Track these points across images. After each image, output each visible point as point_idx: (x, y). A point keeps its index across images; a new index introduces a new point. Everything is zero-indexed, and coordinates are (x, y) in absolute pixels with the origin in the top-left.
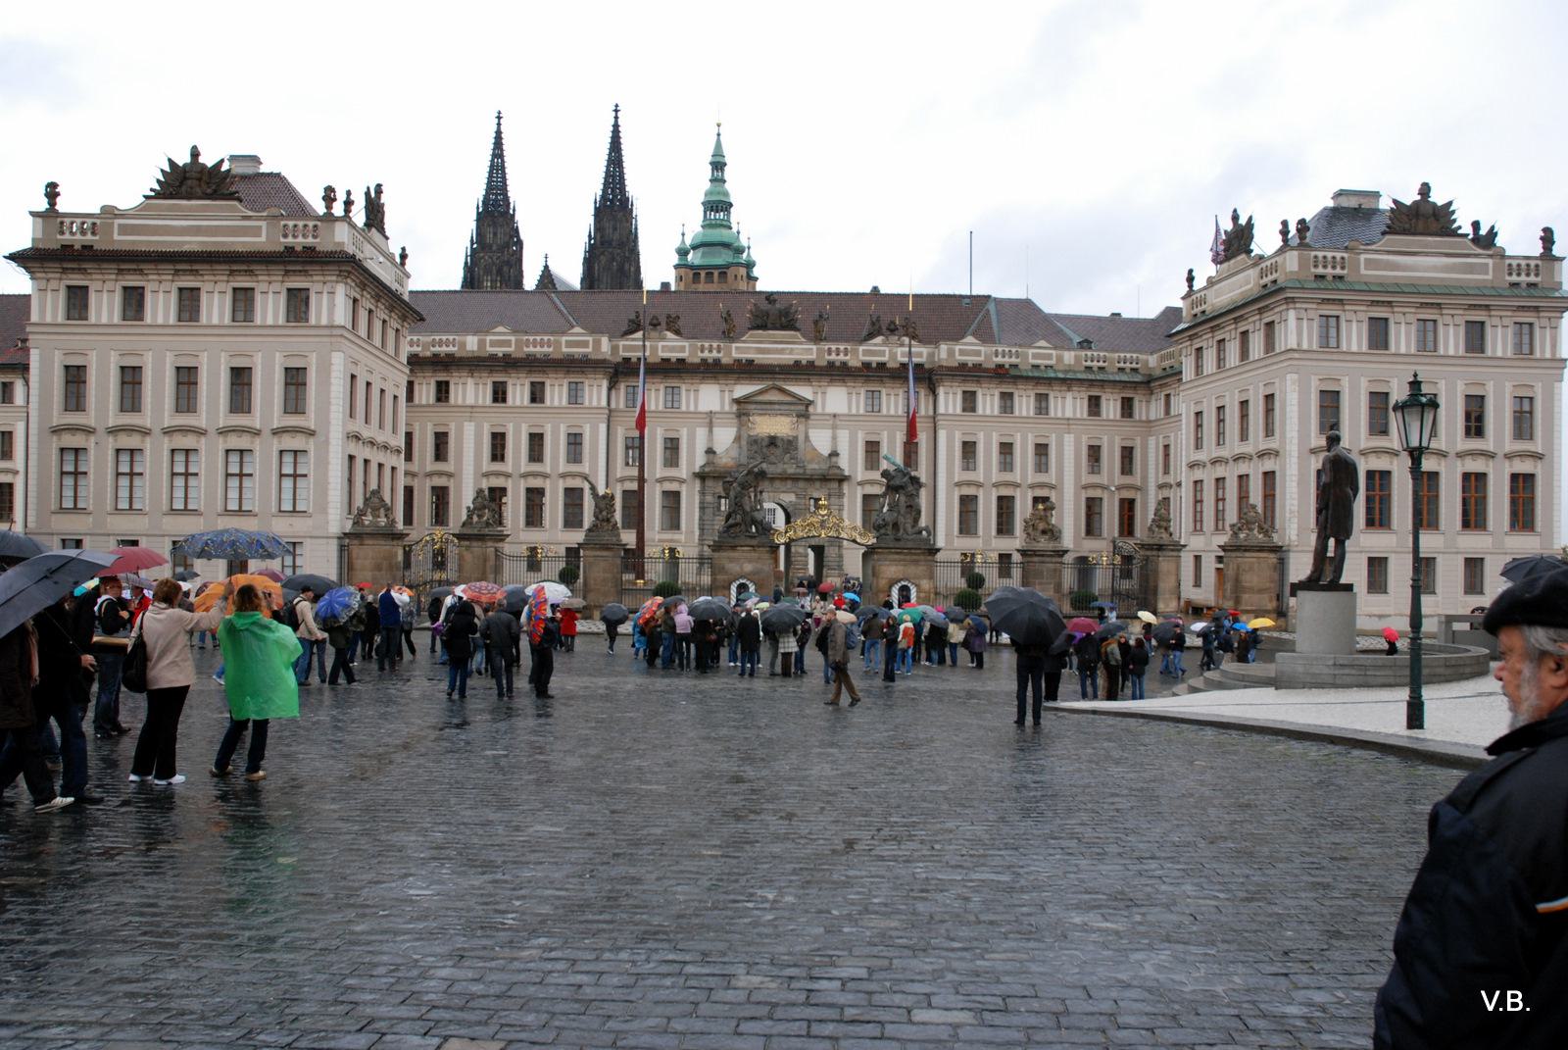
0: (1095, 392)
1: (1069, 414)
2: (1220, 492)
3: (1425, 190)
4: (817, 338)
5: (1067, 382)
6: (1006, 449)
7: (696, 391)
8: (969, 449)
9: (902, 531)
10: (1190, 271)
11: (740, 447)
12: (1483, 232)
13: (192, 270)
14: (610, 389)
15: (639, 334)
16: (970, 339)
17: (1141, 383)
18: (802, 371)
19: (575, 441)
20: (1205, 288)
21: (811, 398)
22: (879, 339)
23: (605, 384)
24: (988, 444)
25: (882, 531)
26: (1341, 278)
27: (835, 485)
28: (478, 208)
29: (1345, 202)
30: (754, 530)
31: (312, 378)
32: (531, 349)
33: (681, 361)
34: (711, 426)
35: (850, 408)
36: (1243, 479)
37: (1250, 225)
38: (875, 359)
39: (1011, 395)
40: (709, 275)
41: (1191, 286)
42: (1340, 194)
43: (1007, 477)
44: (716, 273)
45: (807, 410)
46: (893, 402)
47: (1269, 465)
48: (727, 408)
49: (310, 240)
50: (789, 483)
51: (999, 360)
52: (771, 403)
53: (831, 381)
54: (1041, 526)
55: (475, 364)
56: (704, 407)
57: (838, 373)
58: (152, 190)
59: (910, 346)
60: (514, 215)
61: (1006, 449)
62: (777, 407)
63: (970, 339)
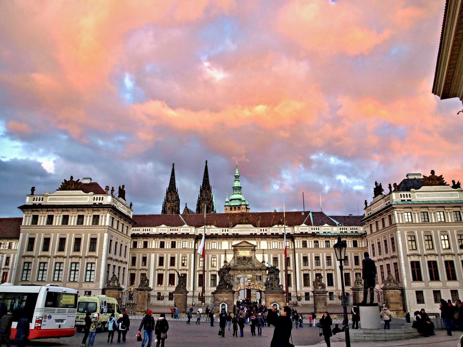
2: (382, 270)
3: (433, 172)
6: (317, 258)
7: (221, 243)
8: (305, 259)
9: (274, 286)
10: (366, 201)
11: (235, 260)
12: (456, 183)
13: (67, 210)
14: (195, 243)
15: (203, 227)
16: (303, 225)
17: (359, 236)
18: (253, 236)
20: (370, 206)
22: (276, 226)
23: (193, 241)
25: (268, 286)
26: (410, 200)
28: (167, 190)
29: (410, 177)
30: (227, 287)
31: (98, 241)
32: (172, 232)
33: (217, 234)
34: (226, 254)
36: (388, 265)
37: (380, 186)
38: (275, 232)
39: (317, 242)
40: (235, 208)
41: (366, 205)
42: (407, 176)
43: (318, 267)
44: (237, 208)
45: (255, 248)
47: (395, 260)
48: (230, 248)
49: (101, 201)
50: (250, 271)
51: (313, 231)
53: (262, 239)
54: (319, 283)
55: (155, 236)
56: (223, 248)
58: (59, 188)
59: (285, 228)
60: (177, 192)
61: (317, 258)
62: (245, 247)
63: (303, 225)
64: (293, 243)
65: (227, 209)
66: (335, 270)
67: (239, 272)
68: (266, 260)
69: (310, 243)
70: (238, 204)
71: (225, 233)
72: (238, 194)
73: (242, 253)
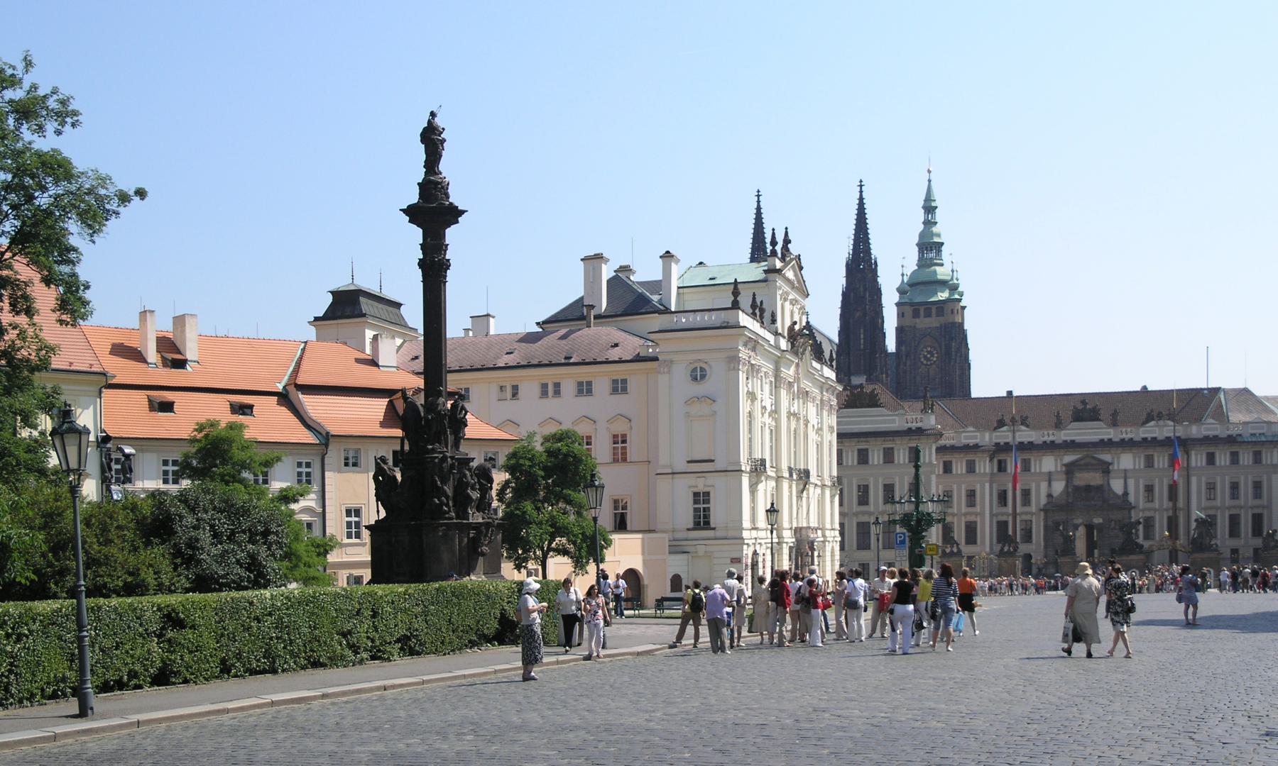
4: (1114, 423)
6: (1235, 487)
7: (1041, 461)
8: (1211, 487)
15: (1005, 428)
19: (971, 495)
21: (1110, 461)
22: (1152, 423)
23: (988, 459)
27: (1126, 512)
35: (1135, 465)
38: (1149, 436)
43: (1235, 502)
44: (934, 311)
48: (1059, 469)
49: (919, 425)
51: (1229, 433)
52: (1087, 465)
61: (1235, 487)
64: (1186, 457)
65: (903, 314)
69: (1222, 458)
73: (1083, 478)
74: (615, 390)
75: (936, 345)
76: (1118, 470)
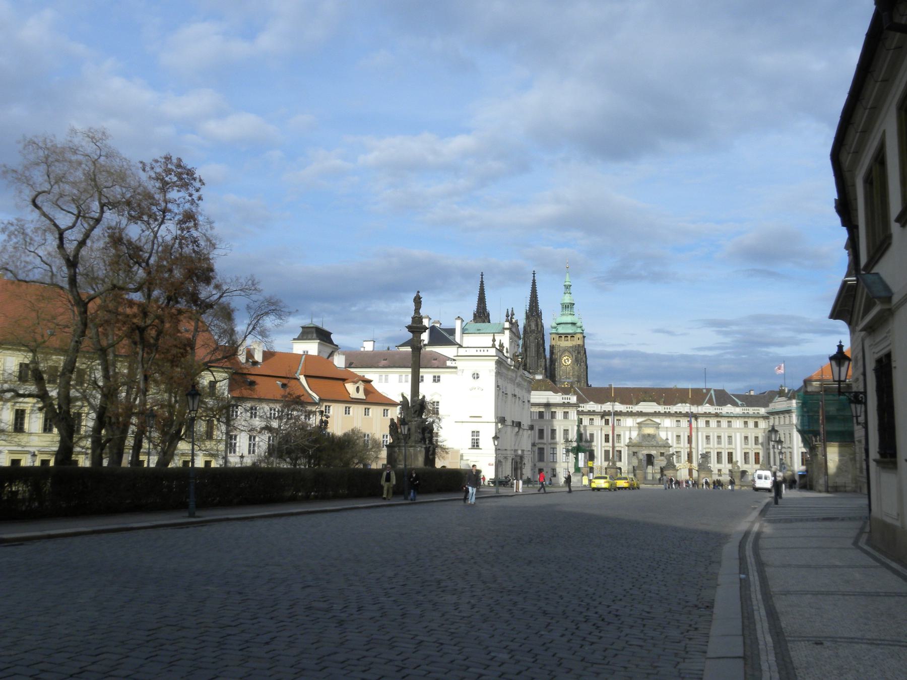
0: (746, 420)
1: (738, 427)
5: (736, 417)
6: (719, 437)
8: (708, 437)
15: (609, 403)
18: (657, 414)
22: (680, 405)
24: (713, 435)
33: (621, 411)
34: (630, 431)
38: (678, 411)
46: (684, 422)
47: (790, 450)
49: (568, 401)
51: (716, 411)
57: (667, 415)
61: (719, 437)
63: (707, 405)
66: (735, 449)
67: (644, 448)
68: (670, 438)
70: (570, 331)
71: (629, 410)
72: (570, 314)
74: (434, 381)
75: (571, 356)
76: (664, 427)
